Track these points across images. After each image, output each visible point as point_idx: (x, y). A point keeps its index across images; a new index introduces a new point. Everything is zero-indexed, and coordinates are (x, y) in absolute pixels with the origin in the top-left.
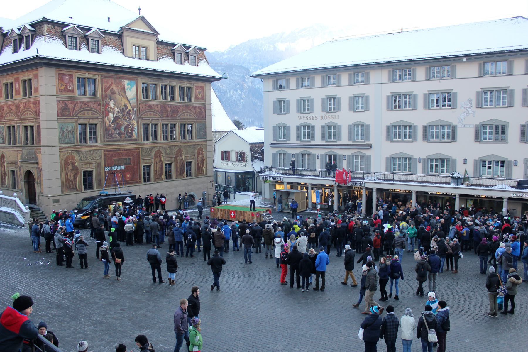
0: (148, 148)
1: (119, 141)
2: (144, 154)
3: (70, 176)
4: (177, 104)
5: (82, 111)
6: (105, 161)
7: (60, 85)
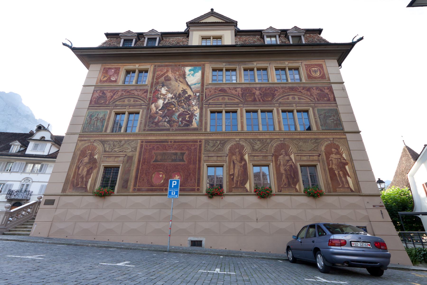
0: (217, 140)
1: (168, 130)
2: (209, 147)
5: (122, 98)
7: (103, 77)
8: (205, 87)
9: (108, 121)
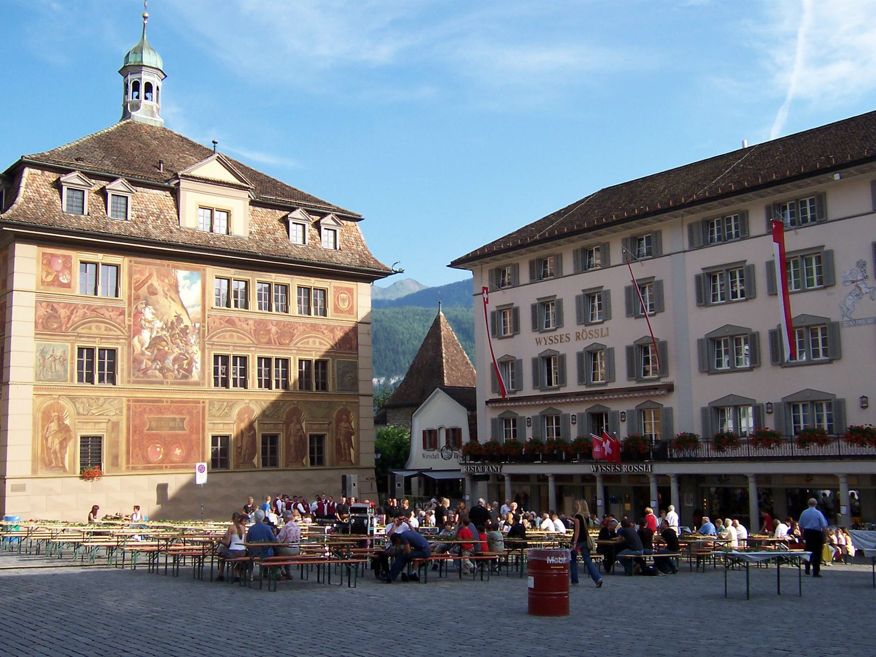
0: (222, 401)
1: (161, 383)
2: (214, 411)
3: (53, 442)
4: (292, 320)
5: (85, 321)
6: (128, 419)
7: (44, 274)
8: (207, 313)
9: (72, 363)
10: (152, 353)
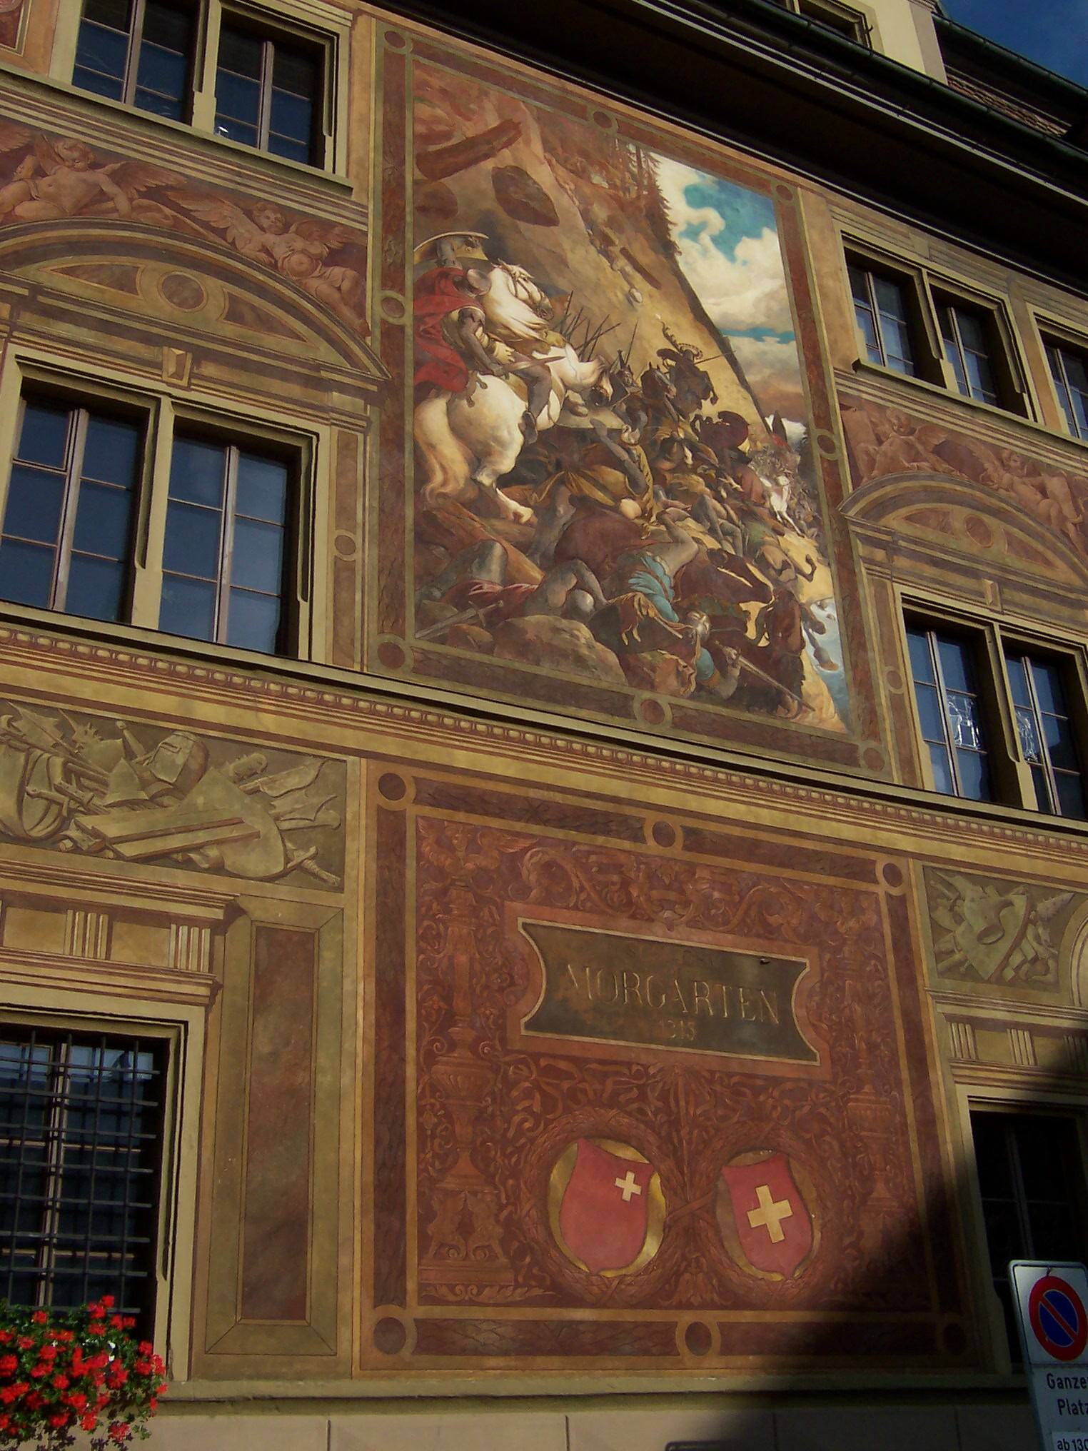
1: (618, 706)
10: (545, 511)
